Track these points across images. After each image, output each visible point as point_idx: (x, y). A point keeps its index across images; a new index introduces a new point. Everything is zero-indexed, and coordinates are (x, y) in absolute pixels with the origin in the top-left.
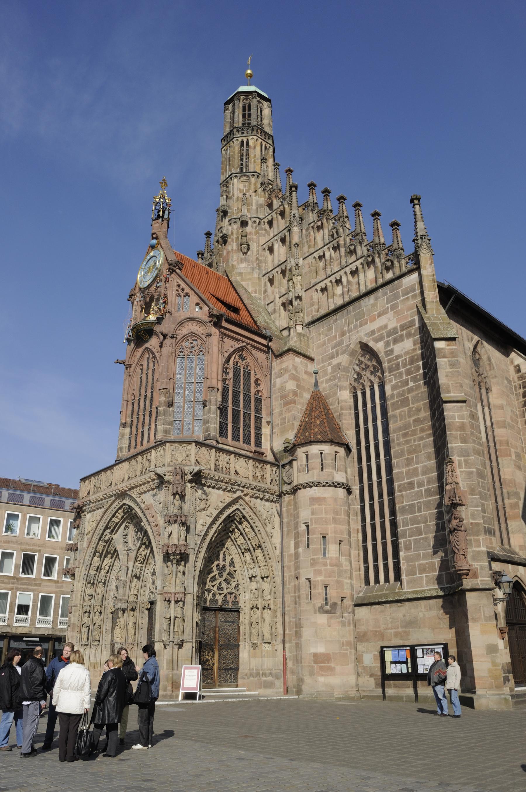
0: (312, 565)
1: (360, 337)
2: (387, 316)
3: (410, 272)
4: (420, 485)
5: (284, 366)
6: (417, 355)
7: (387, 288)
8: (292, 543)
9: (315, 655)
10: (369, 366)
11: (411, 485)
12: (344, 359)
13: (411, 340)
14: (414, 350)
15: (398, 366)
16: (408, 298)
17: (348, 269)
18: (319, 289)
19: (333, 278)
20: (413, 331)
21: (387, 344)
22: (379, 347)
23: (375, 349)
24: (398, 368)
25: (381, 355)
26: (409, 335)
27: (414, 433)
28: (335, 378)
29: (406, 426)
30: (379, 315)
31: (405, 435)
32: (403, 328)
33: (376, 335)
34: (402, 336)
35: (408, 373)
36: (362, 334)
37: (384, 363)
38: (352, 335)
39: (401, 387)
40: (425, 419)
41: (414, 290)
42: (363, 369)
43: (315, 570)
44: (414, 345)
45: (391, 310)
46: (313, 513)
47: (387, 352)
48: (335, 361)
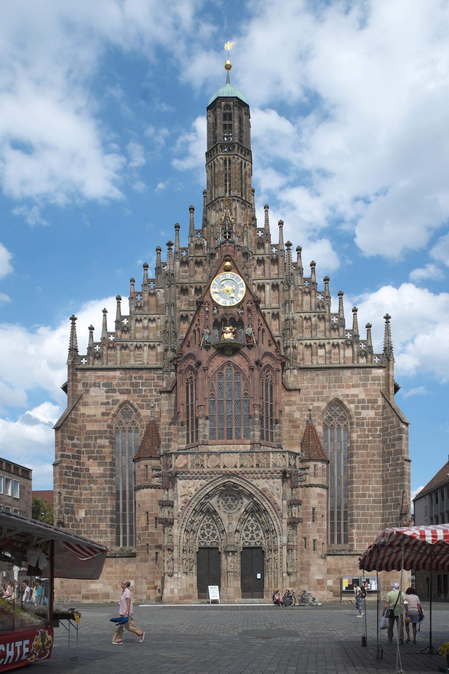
0: (318, 532)
1: (338, 395)
2: (359, 389)
3: (379, 367)
6: (376, 422)
7: (361, 371)
9: (318, 580)
10: (338, 415)
12: (323, 405)
13: (374, 411)
14: (375, 418)
15: (363, 424)
16: (375, 383)
17: (331, 341)
18: (304, 344)
19: (317, 342)
20: (376, 406)
21: (357, 408)
22: (352, 407)
23: (348, 407)
24: (363, 426)
25: (352, 413)
26: (373, 408)
28: (315, 415)
30: (354, 386)
33: (350, 398)
34: (368, 406)
36: (339, 393)
37: (354, 419)
38: (331, 391)
39: (364, 438)
41: (379, 381)
42: (333, 415)
43: (319, 535)
44: (376, 415)
45: (363, 387)
46: (319, 503)
47: (356, 412)
48: (316, 404)
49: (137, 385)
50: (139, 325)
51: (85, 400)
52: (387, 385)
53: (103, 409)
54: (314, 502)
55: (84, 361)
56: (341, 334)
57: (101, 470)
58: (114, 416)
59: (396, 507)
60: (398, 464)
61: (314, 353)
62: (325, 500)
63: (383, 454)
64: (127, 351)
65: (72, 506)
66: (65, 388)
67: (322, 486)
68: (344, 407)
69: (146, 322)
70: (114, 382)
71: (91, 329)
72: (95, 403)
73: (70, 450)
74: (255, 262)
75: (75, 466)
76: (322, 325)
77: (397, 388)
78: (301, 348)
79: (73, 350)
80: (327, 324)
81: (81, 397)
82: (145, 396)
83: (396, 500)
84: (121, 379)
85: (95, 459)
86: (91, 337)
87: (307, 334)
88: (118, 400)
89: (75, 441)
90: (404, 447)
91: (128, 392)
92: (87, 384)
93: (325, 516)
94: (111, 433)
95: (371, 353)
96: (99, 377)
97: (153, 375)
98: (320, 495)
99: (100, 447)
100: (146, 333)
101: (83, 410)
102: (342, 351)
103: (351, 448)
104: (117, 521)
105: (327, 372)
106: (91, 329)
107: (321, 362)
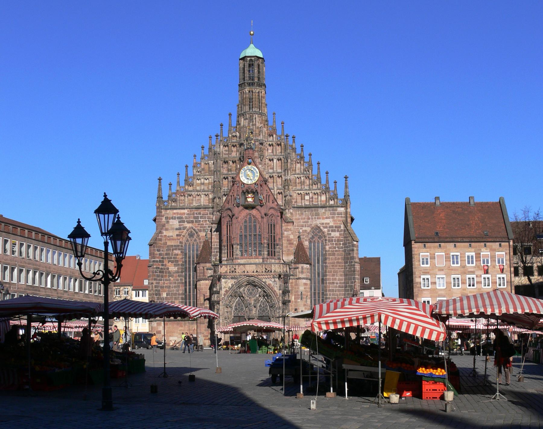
4: (337, 283)
5: (289, 227)
7: (331, 209)
8: (293, 297)
11: (333, 283)
12: (308, 229)
15: (332, 241)
17: (313, 191)
19: (305, 192)
21: (329, 231)
26: (338, 231)
27: (336, 266)
29: (334, 263)
30: (326, 218)
31: (332, 266)
32: (336, 227)
35: (336, 244)
40: (340, 263)
48: (304, 229)
49: (197, 218)
50: (199, 182)
51: (166, 227)
52: (346, 217)
53: (177, 232)
54: (302, 288)
55: (166, 204)
56: (319, 187)
57: (176, 269)
58: (184, 236)
59: (351, 291)
60: (352, 265)
61: (303, 198)
62: (309, 286)
63: (344, 260)
64: (192, 197)
65: (159, 291)
66: (155, 220)
67: (307, 279)
68: (321, 230)
69: (202, 180)
70: (184, 217)
71: (170, 184)
72: (173, 229)
73: (158, 258)
74: (267, 145)
75: (160, 267)
76: (307, 182)
77: (352, 220)
78: (295, 195)
79: (160, 197)
80: (311, 181)
81: (164, 225)
82: (202, 224)
83: (351, 286)
84: (188, 214)
85: (172, 262)
86: (170, 189)
87: (299, 187)
88: (186, 227)
89: (161, 252)
90: (355, 255)
91: (192, 222)
92: (168, 217)
93: (309, 296)
94: (182, 246)
95: (337, 198)
96: (175, 213)
97: (207, 211)
98: (305, 284)
99: (175, 255)
100: (202, 187)
101: (165, 233)
102: (319, 197)
103: (324, 255)
104: (186, 299)
105: (311, 209)
106: (170, 184)
107: (307, 203)
